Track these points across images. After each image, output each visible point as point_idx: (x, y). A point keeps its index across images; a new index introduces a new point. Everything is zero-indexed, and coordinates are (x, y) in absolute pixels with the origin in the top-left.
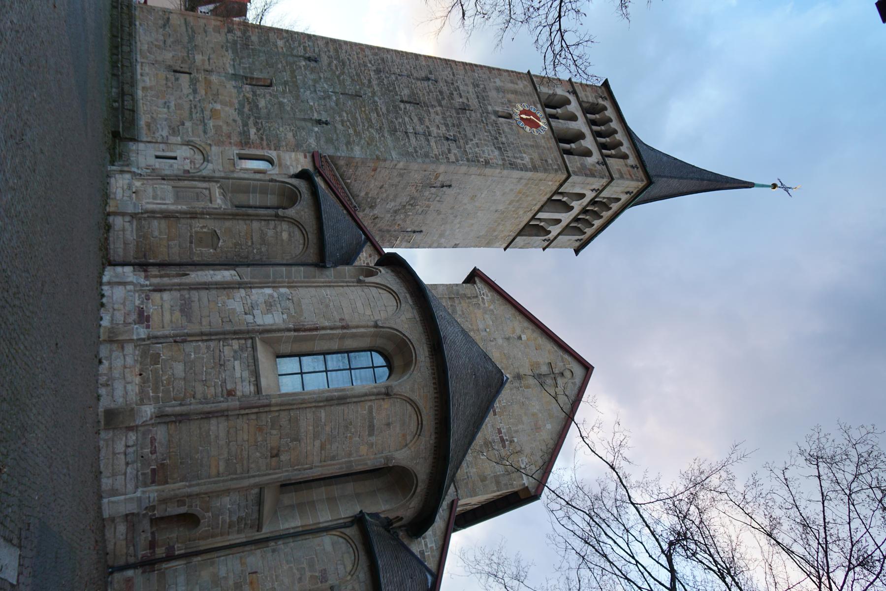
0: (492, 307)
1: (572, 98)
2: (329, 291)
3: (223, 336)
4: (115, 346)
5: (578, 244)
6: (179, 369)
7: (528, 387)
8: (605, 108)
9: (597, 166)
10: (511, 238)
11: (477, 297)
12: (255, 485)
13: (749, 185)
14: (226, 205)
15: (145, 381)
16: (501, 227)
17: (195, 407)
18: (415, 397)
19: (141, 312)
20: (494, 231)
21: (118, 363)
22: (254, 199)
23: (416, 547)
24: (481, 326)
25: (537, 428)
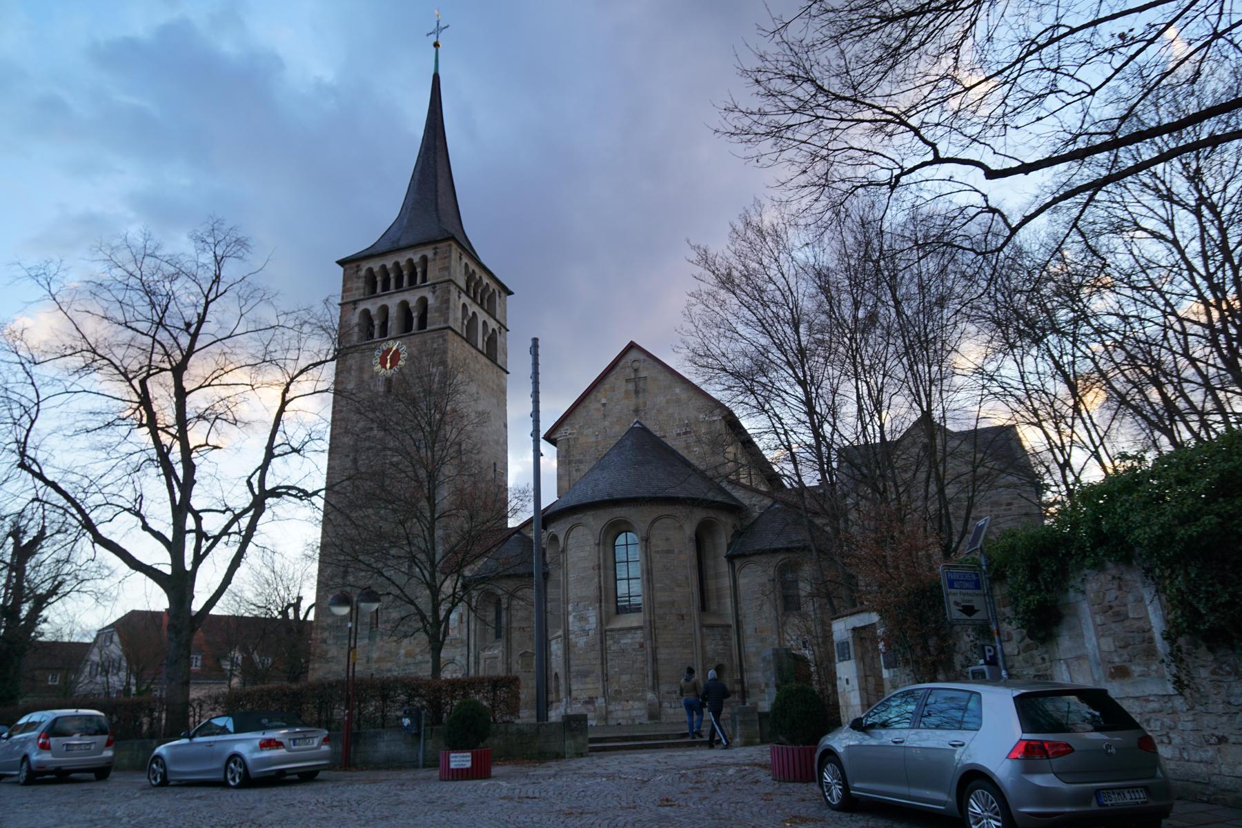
0: (577, 427)
1: (362, 306)
2: (571, 575)
3: (604, 650)
4: (609, 717)
5: (503, 294)
6: (625, 678)
7: (645, 404)
8: (370, 270)
9: (437, 293)
10: (499, 370)
11: (568, 439)
12: (701, 630)
13: (436, 79)
14: (499, 646)
15: (632, 698)
16: (490, 384)
17: (649, 668)
18: (650, 520)
19: (586, 703)
20: (493, 389)
21: (620, 714)
23: (756, 512)
24: (593, 439)
25: (678, 401)
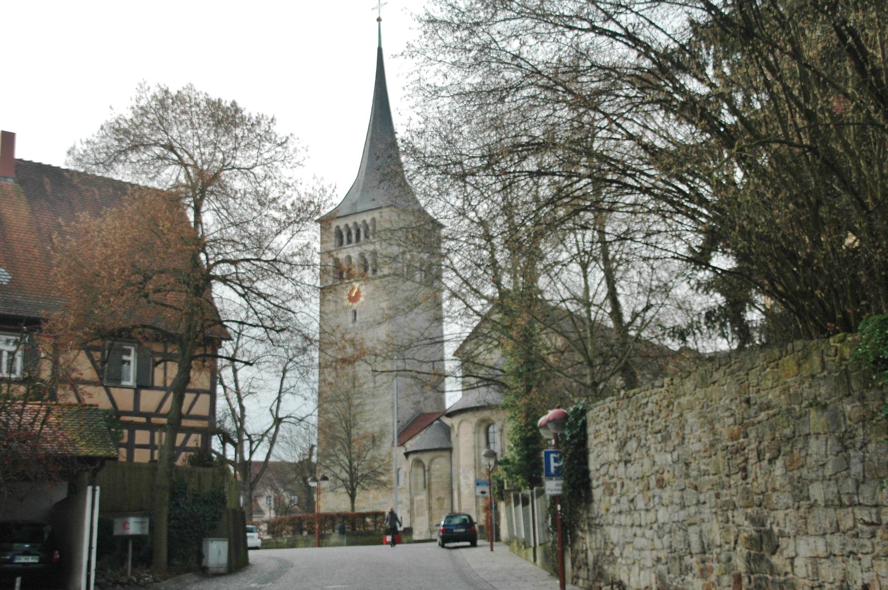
8: (338, 227)
13: (380, 51)
22: (421, 480)
